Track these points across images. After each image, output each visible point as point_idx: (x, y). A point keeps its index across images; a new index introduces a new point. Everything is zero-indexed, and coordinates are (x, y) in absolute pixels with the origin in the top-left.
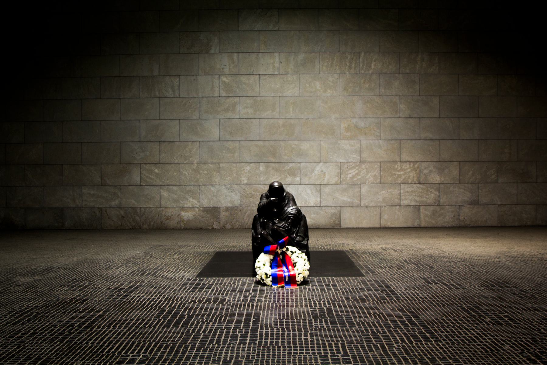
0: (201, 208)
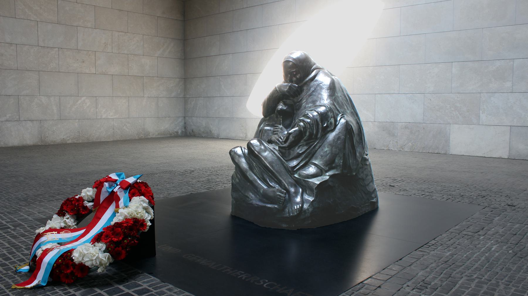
0: (376, 123)
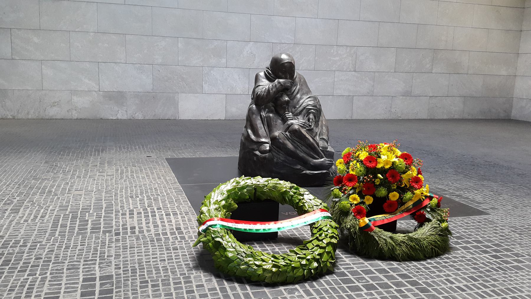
0: (102, 93)
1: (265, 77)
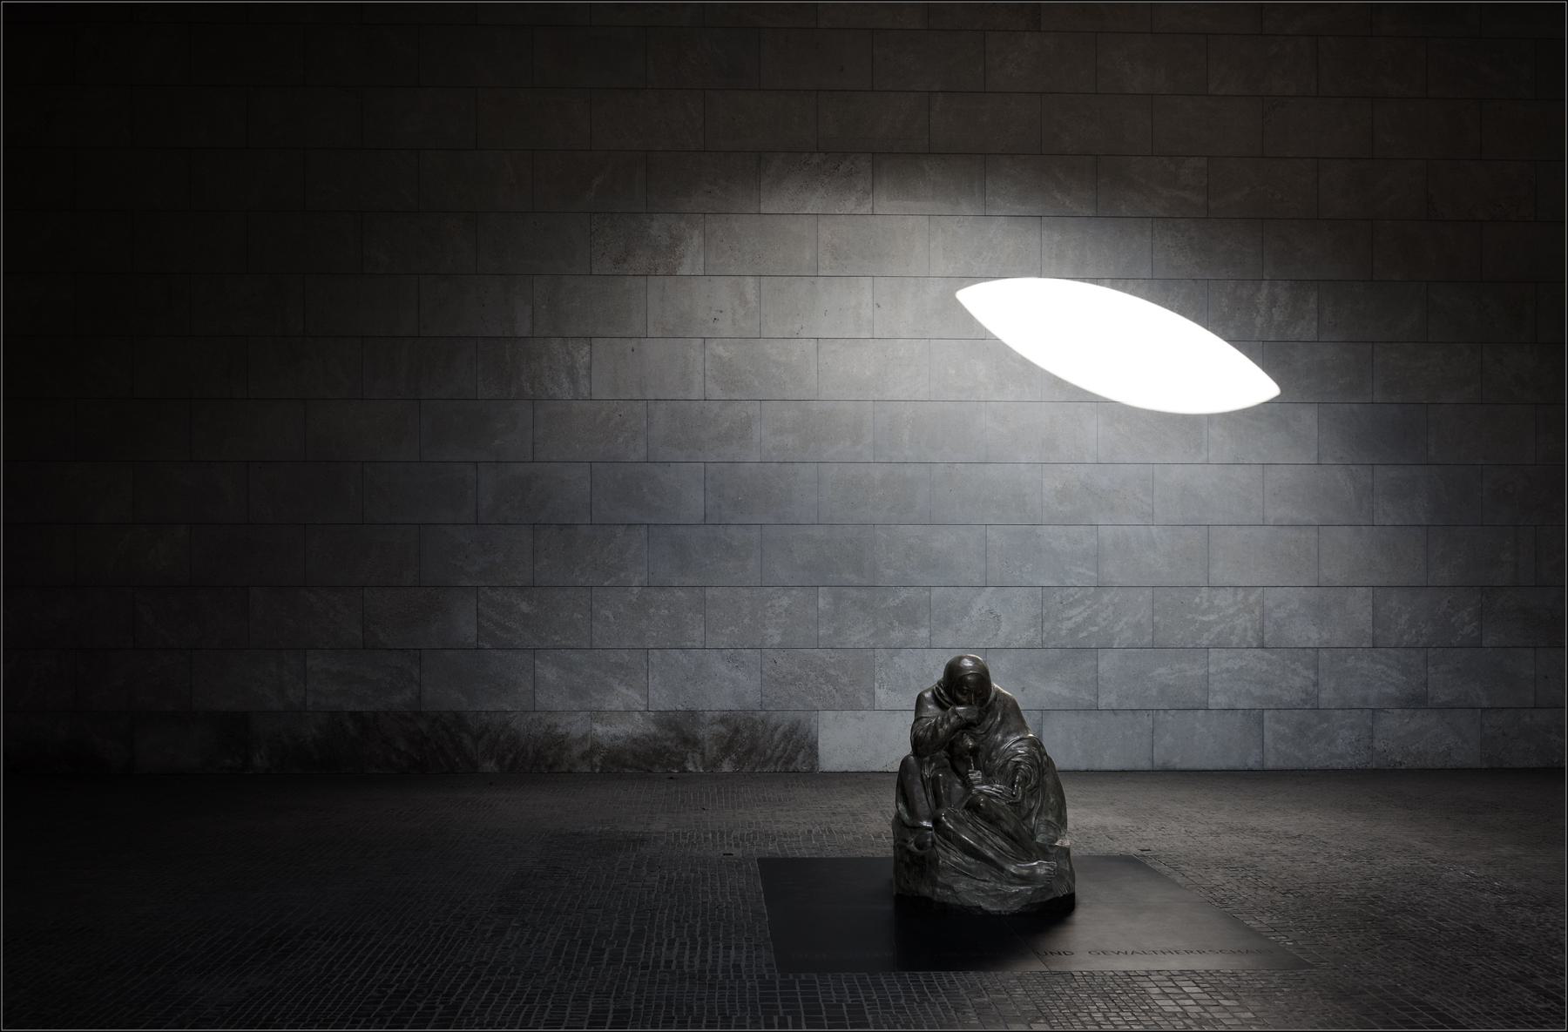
1: (933, 701)
